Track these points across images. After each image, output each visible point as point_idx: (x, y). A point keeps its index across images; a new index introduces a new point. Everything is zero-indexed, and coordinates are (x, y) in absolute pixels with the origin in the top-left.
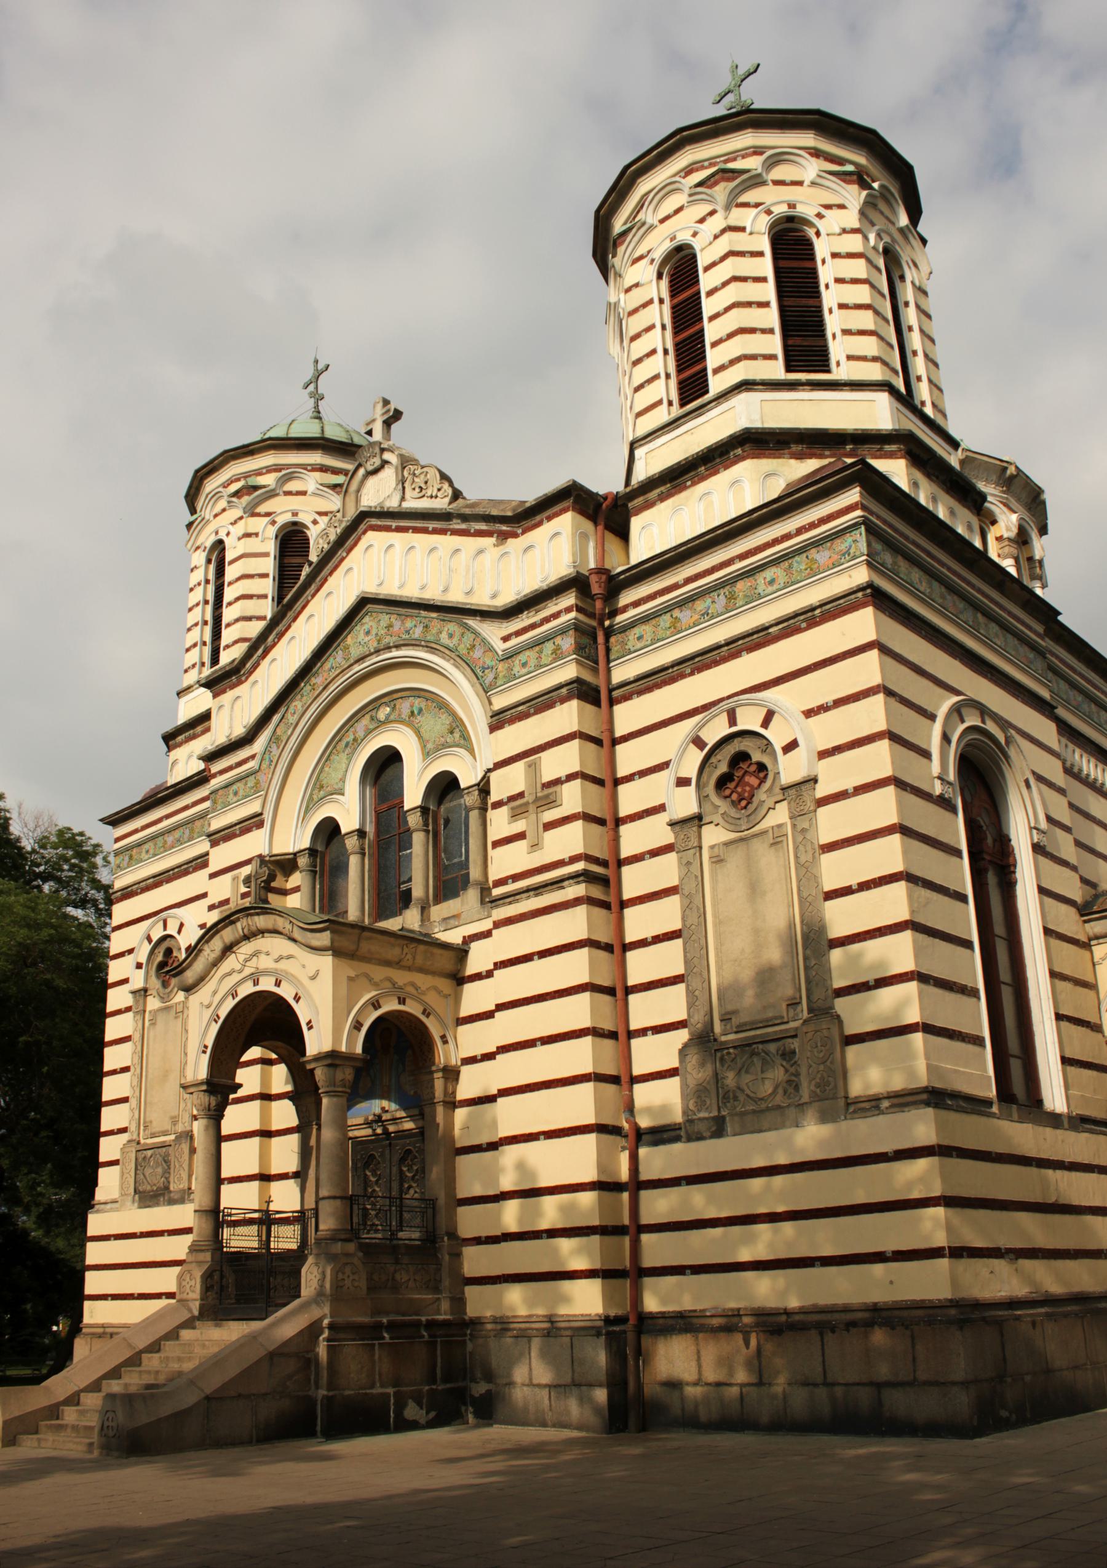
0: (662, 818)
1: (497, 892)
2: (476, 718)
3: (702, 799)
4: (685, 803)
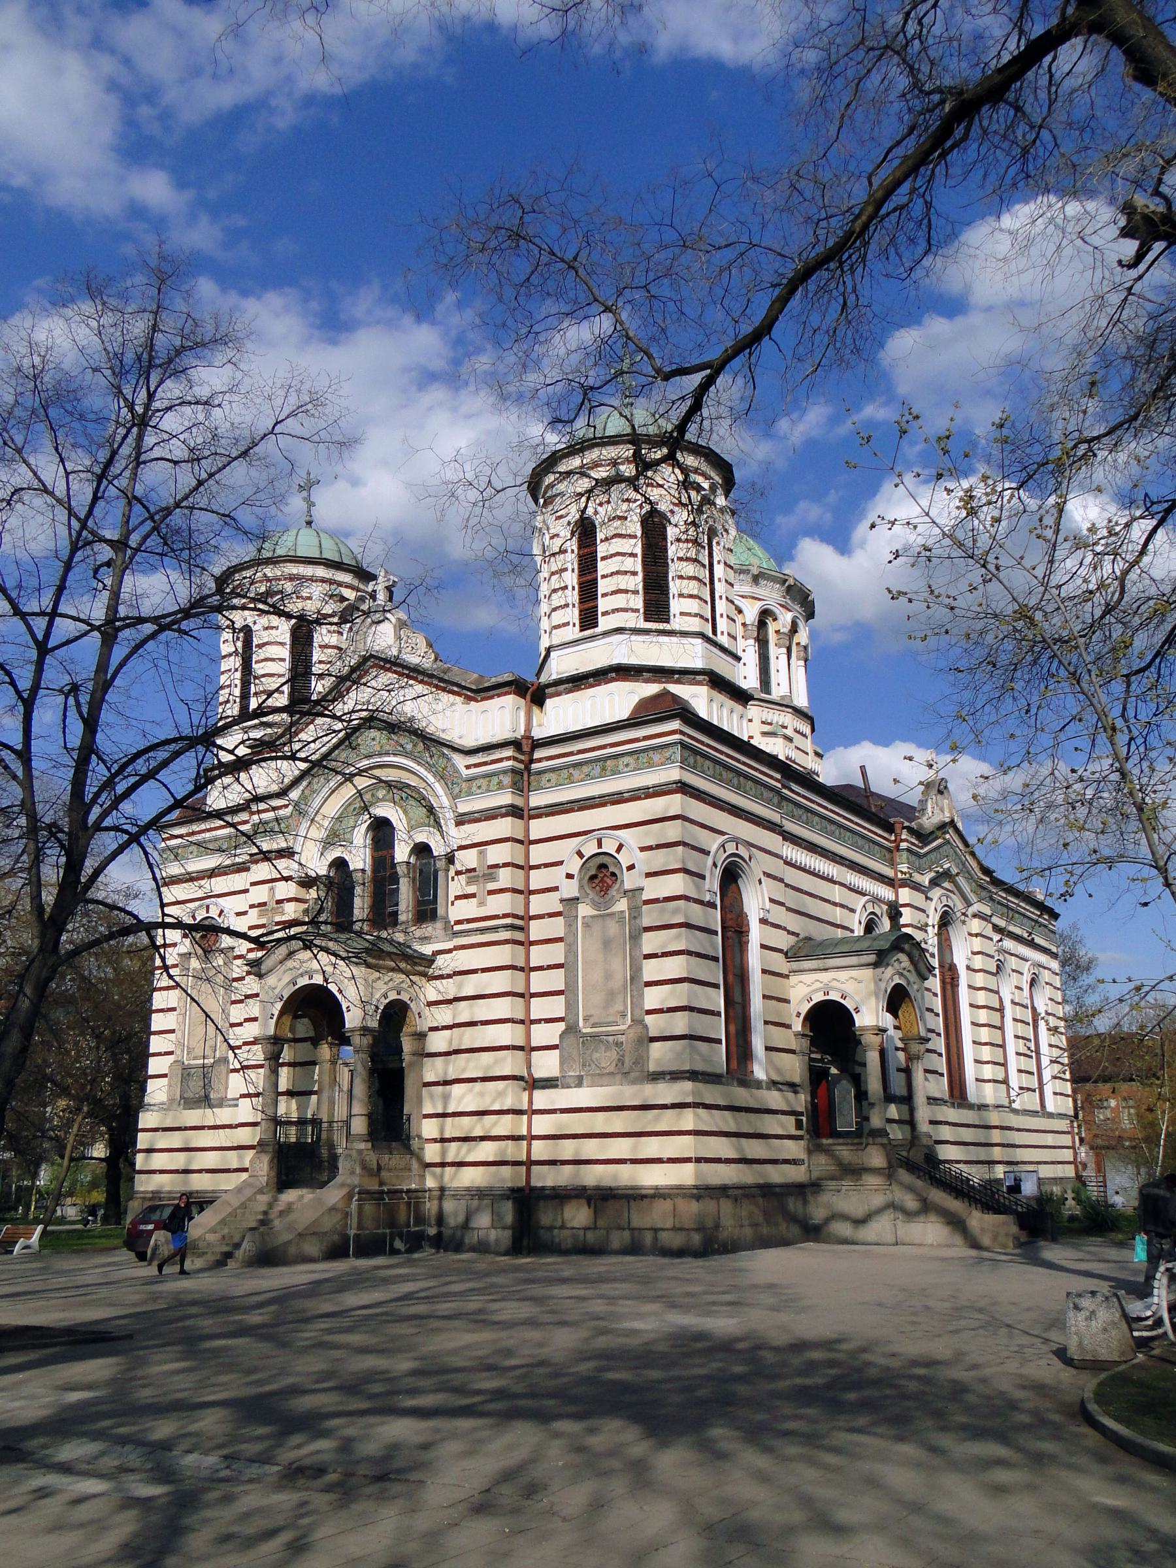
0: (555, 896)
1: (457, 928)
2: (447, 818)
3: (581, 887)
4: (570, 889)
